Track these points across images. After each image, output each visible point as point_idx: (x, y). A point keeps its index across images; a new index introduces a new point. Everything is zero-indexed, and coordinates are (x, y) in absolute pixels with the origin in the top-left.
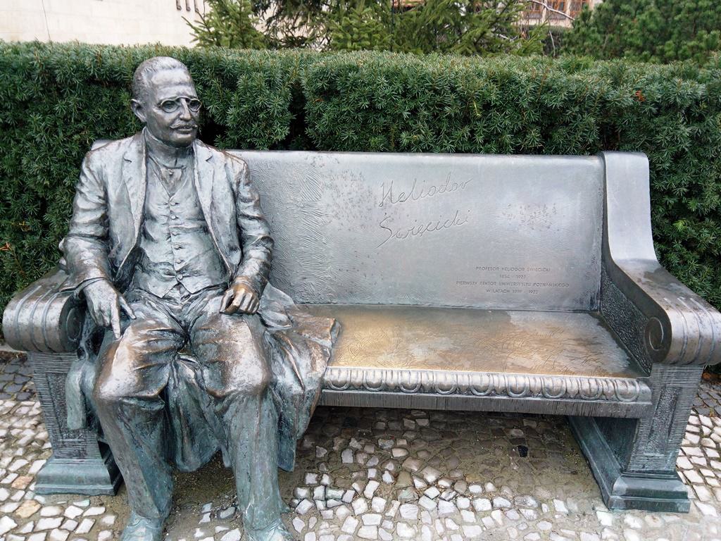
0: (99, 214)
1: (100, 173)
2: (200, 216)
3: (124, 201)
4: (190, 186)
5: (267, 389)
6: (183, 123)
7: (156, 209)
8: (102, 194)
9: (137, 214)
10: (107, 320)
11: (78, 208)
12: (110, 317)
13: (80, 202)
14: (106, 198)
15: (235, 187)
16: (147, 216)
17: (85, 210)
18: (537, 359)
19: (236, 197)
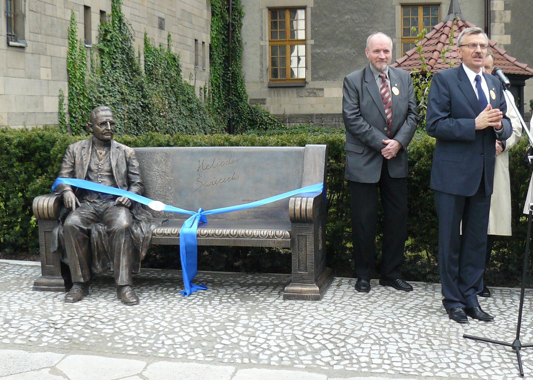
0: (71, 170)
1: (73, 152)
2: (111, 171)
3: (82, 165)
4: (108, 158)
5: (128, 230)
6: (107, 131)
7: (94, 167)
8: (73, 162)
9: (86, 168)
10: (70, 205)
11: (63, 168)
12: (72, 203)
13: (64, 165)
14: (74, 164)
15: (128, 160)
16: (90, 170)
17: (66, 168)
18: (494, 97)
19: (128, 164)
